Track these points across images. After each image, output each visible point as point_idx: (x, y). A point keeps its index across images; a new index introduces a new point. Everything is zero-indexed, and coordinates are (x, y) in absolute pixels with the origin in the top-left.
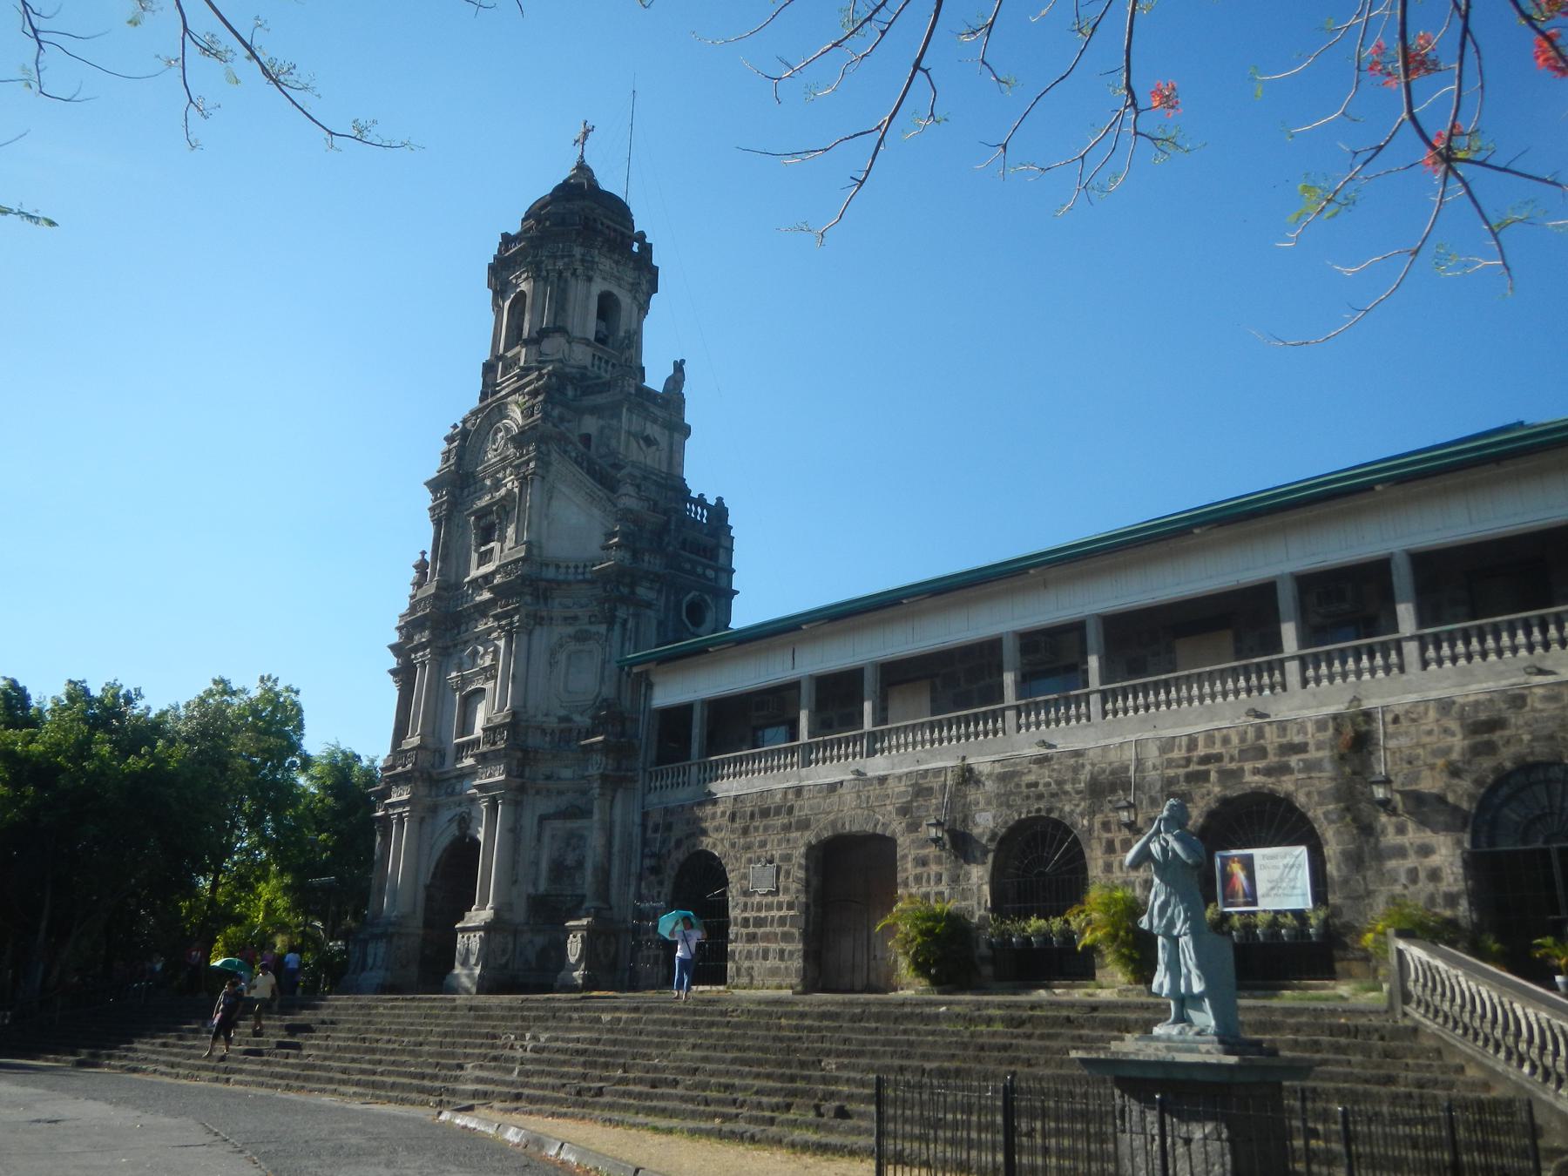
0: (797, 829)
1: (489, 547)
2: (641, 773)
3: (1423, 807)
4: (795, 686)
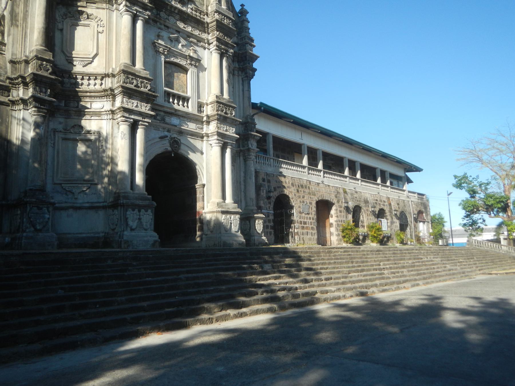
0: (313, 195)
3: (396, 214)
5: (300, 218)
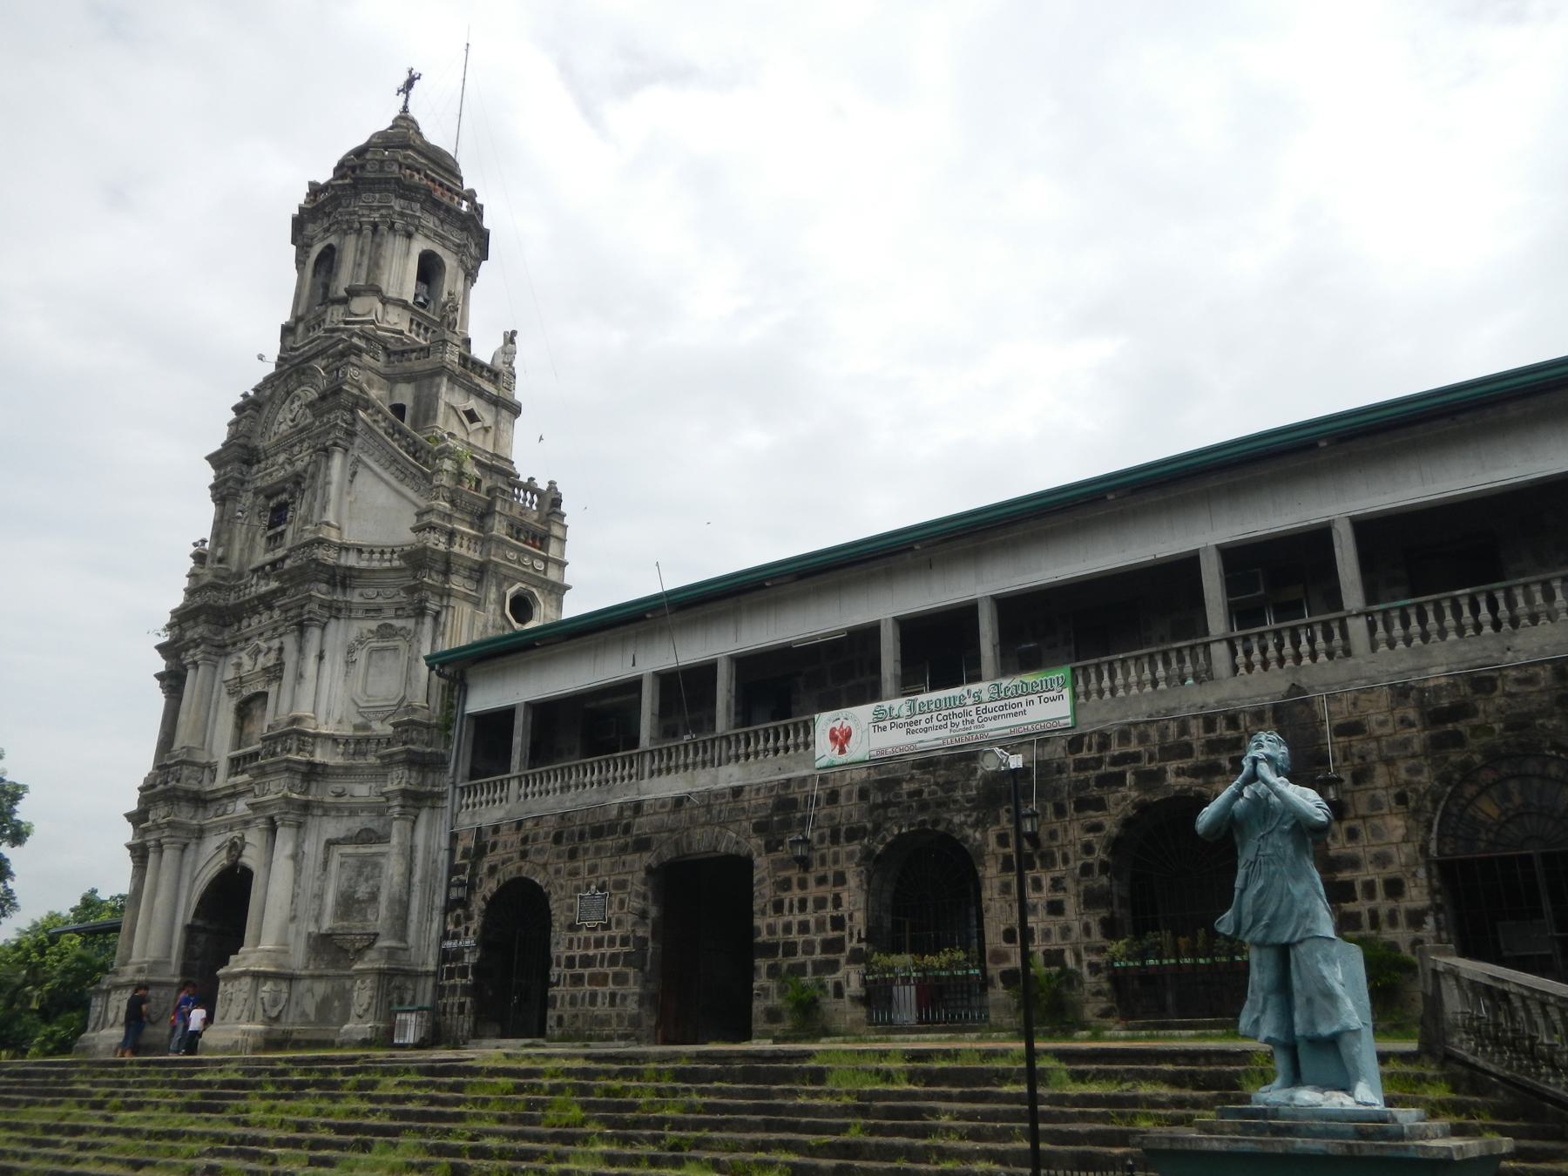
1: (279, 529)
2: (451, 787)
4: (634, 685)
5: (570, 947)
